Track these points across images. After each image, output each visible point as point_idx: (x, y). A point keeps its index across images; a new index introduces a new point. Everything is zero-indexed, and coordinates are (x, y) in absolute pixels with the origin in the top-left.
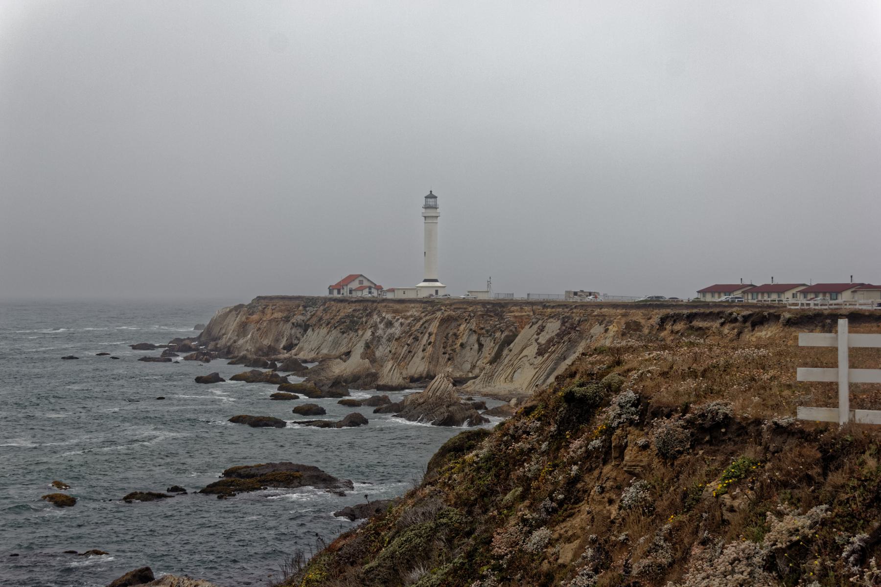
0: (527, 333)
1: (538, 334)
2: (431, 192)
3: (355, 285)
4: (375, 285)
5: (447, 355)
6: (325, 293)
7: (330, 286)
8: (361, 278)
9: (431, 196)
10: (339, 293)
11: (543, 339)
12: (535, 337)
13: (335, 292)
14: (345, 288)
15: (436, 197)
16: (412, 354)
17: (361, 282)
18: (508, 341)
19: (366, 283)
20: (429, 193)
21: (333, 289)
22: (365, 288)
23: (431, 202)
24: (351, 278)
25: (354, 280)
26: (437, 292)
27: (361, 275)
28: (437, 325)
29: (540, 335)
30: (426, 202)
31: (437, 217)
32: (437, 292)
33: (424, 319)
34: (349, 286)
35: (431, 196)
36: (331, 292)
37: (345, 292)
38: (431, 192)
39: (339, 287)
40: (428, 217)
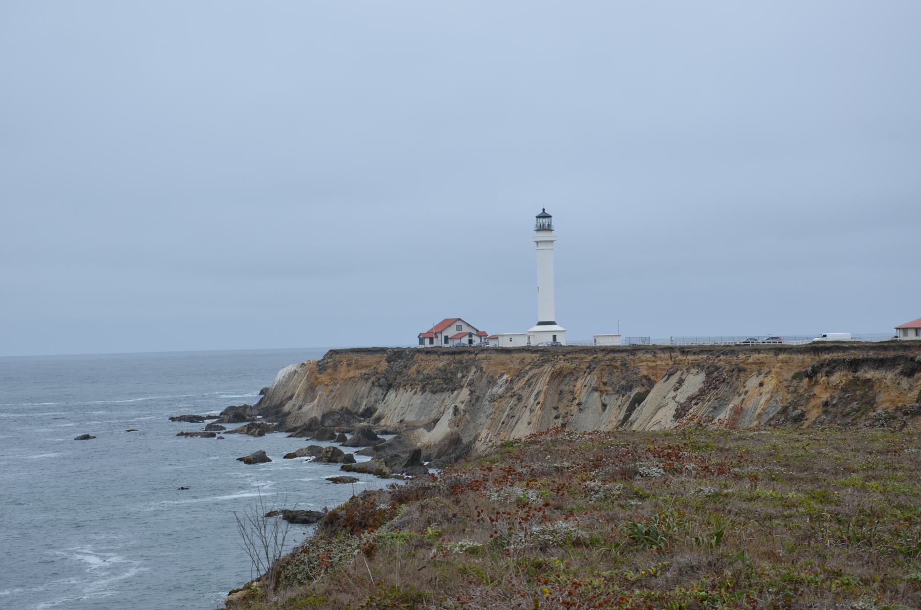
0: (661, 388)
1: (676, 389)
2: (544, 210)
3: (451, 332)
4: (477, 331)
5: (561, 419)
6: (414, 343)
7: (420, 334)
8: (459, 323)
9: (544, 215)
10: (431, 342)
11: (682, 397)
12: (672, 394)
13: (427, 341)
14: (439, 335)
15: (550, 217)
16: (515, 420)
17: (459, 328)
18: (639, 399)
19: (465, 329)
20: (542, 211)
21: (424, 338)
22: (464, 335)
23: (545, 221)
24: (448, 323)
25: (450, 326)
26: (554, 337)
27: (459, 319)
28: (547, 381)
29: (679, 391)
30: (538, 223)
31: (552, 241)
32: (554, 337)
33: (530, 374)
34: (444, 334)
35: (544, 215)
36: (421, 341)
37: (438, 342)
38: (544, 210)
39: (431, 336)
40: (541, 241)
